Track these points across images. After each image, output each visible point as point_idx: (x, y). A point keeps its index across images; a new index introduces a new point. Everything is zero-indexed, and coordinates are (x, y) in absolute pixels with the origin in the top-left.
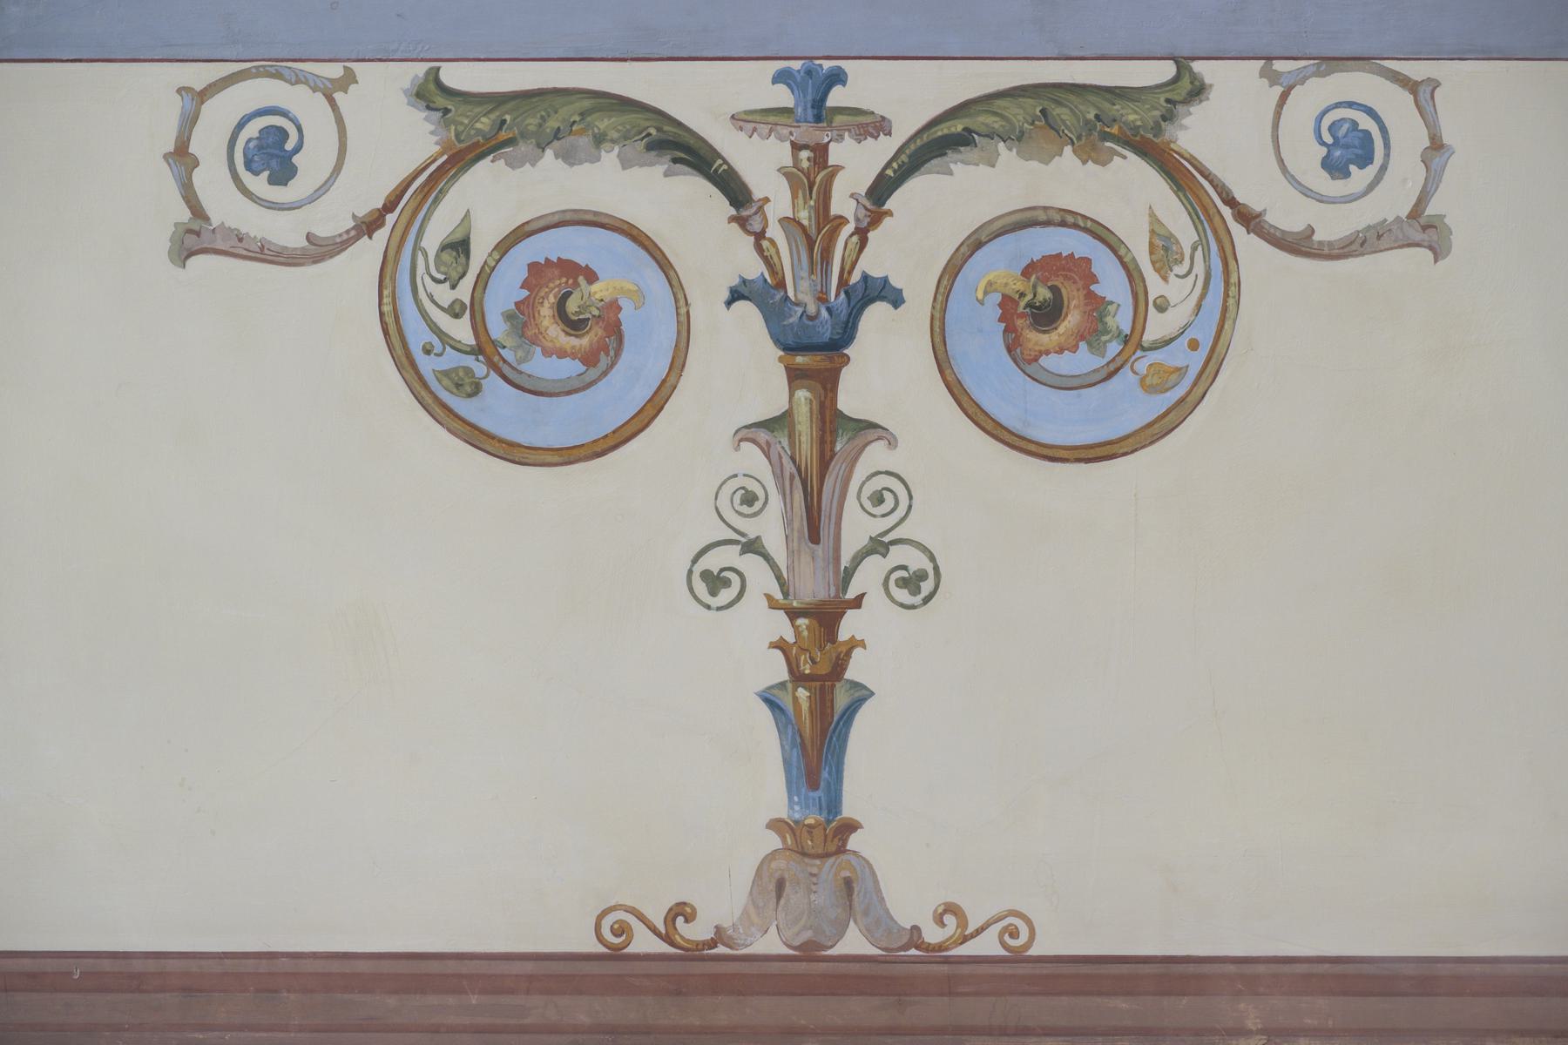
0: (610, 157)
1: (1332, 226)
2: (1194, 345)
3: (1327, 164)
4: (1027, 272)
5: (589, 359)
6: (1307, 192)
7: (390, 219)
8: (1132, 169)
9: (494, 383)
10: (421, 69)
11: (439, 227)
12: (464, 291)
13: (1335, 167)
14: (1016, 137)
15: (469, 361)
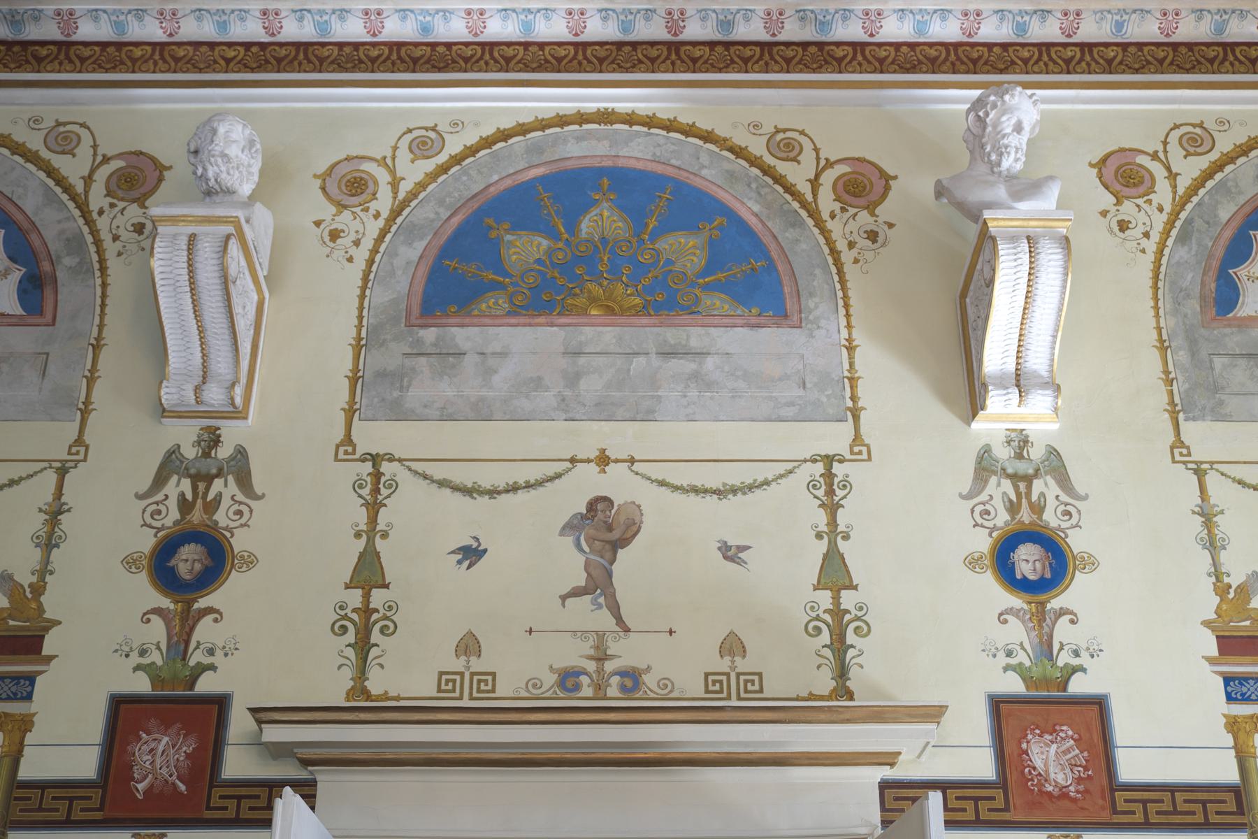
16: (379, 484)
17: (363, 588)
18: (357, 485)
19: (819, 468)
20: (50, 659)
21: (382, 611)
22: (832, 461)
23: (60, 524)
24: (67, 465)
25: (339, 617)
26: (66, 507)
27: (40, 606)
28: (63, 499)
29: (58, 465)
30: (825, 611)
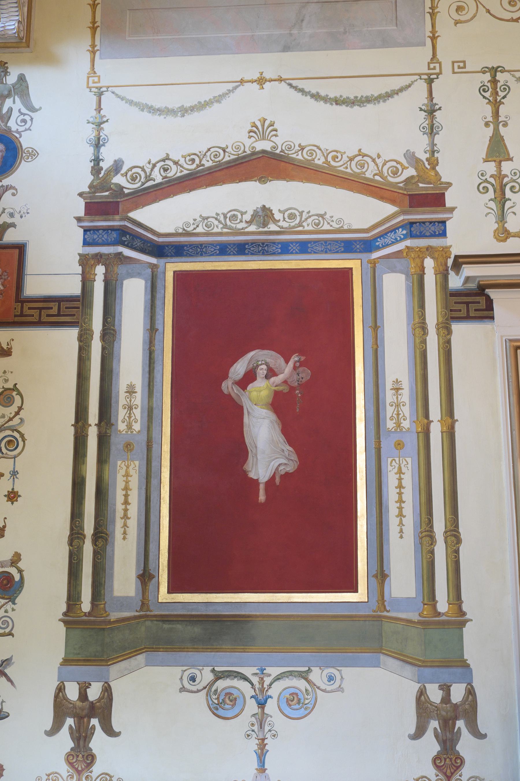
0: (236, 679)
1: (329, 688)
2: (311, 704)
3: (328, 680)
4: (290, 695)
5: (232, 705)
6: (325, 684)
7: (208, 687)
8: (303, 681)
9: (220, 709)
10: (212, 668)
11: (213, 689)
12: (216, 697)
13: (329, 681)
14: (287, 677)
15: (217, 706)
16: (497, 88)
17: (495, 161)
18: (483, 89)
19: (487, 77)
20: (452, 210)
21: (510, 176)
22: (496, 71)
23: (436, 118)
24: (432, 77)
25: (482, 181)
26: (437, 107)
27: (437, 174)
28: (435, 101)
29: (426, 77)
30: (491, 177)
